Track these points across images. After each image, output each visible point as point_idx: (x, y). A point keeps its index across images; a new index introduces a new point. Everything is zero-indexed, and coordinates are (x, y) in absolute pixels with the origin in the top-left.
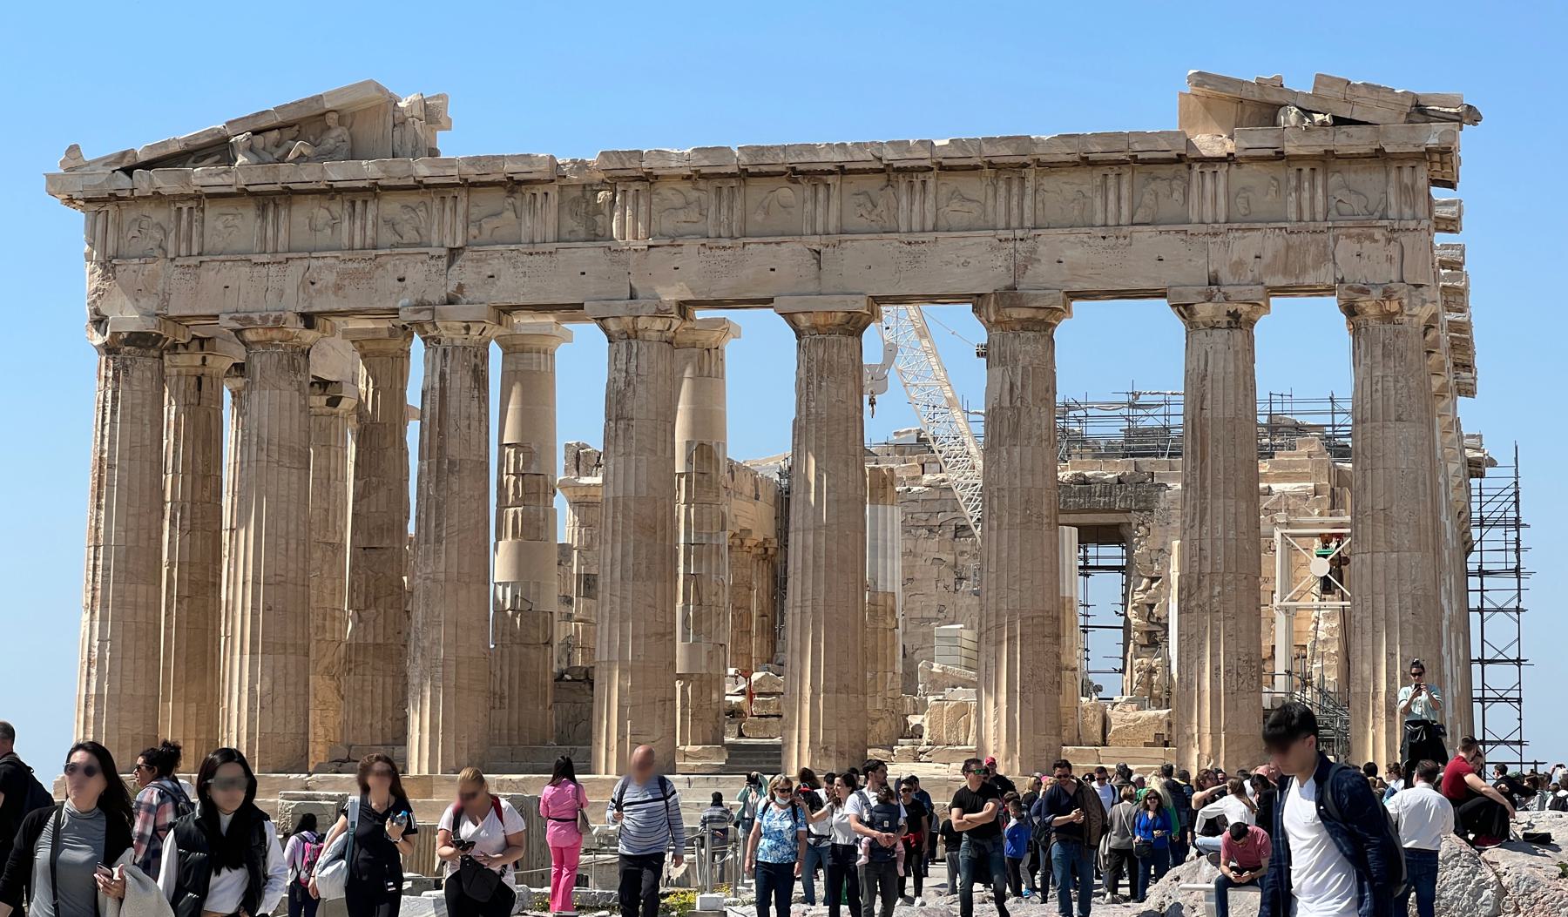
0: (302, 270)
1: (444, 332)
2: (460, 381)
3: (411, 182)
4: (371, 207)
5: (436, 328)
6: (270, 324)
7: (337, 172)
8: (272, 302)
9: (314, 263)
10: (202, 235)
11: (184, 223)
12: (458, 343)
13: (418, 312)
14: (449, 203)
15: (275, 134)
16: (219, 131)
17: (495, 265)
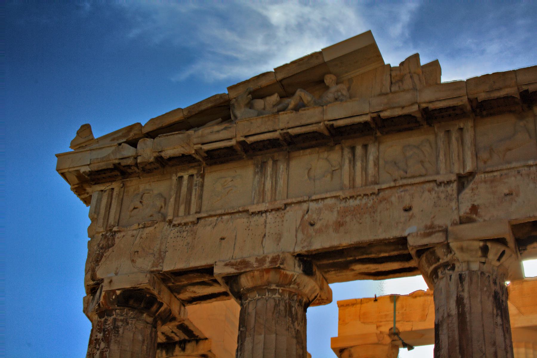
0: (300, 213)
1: (458, 255)
2: (480, 306)
3: (415, 108)
4: (372, 150)
5: (449, 249)
6: (267, 265)
7: (339, 113)
8: (270, 249)
9: (313, 205)
10: (201, 197)
11: (184, 189)
12: (475, 267)
13: (429, 235)
14: (454, 136)
15: (275, 98)
16: (221, 96)
17: (512, 181)
